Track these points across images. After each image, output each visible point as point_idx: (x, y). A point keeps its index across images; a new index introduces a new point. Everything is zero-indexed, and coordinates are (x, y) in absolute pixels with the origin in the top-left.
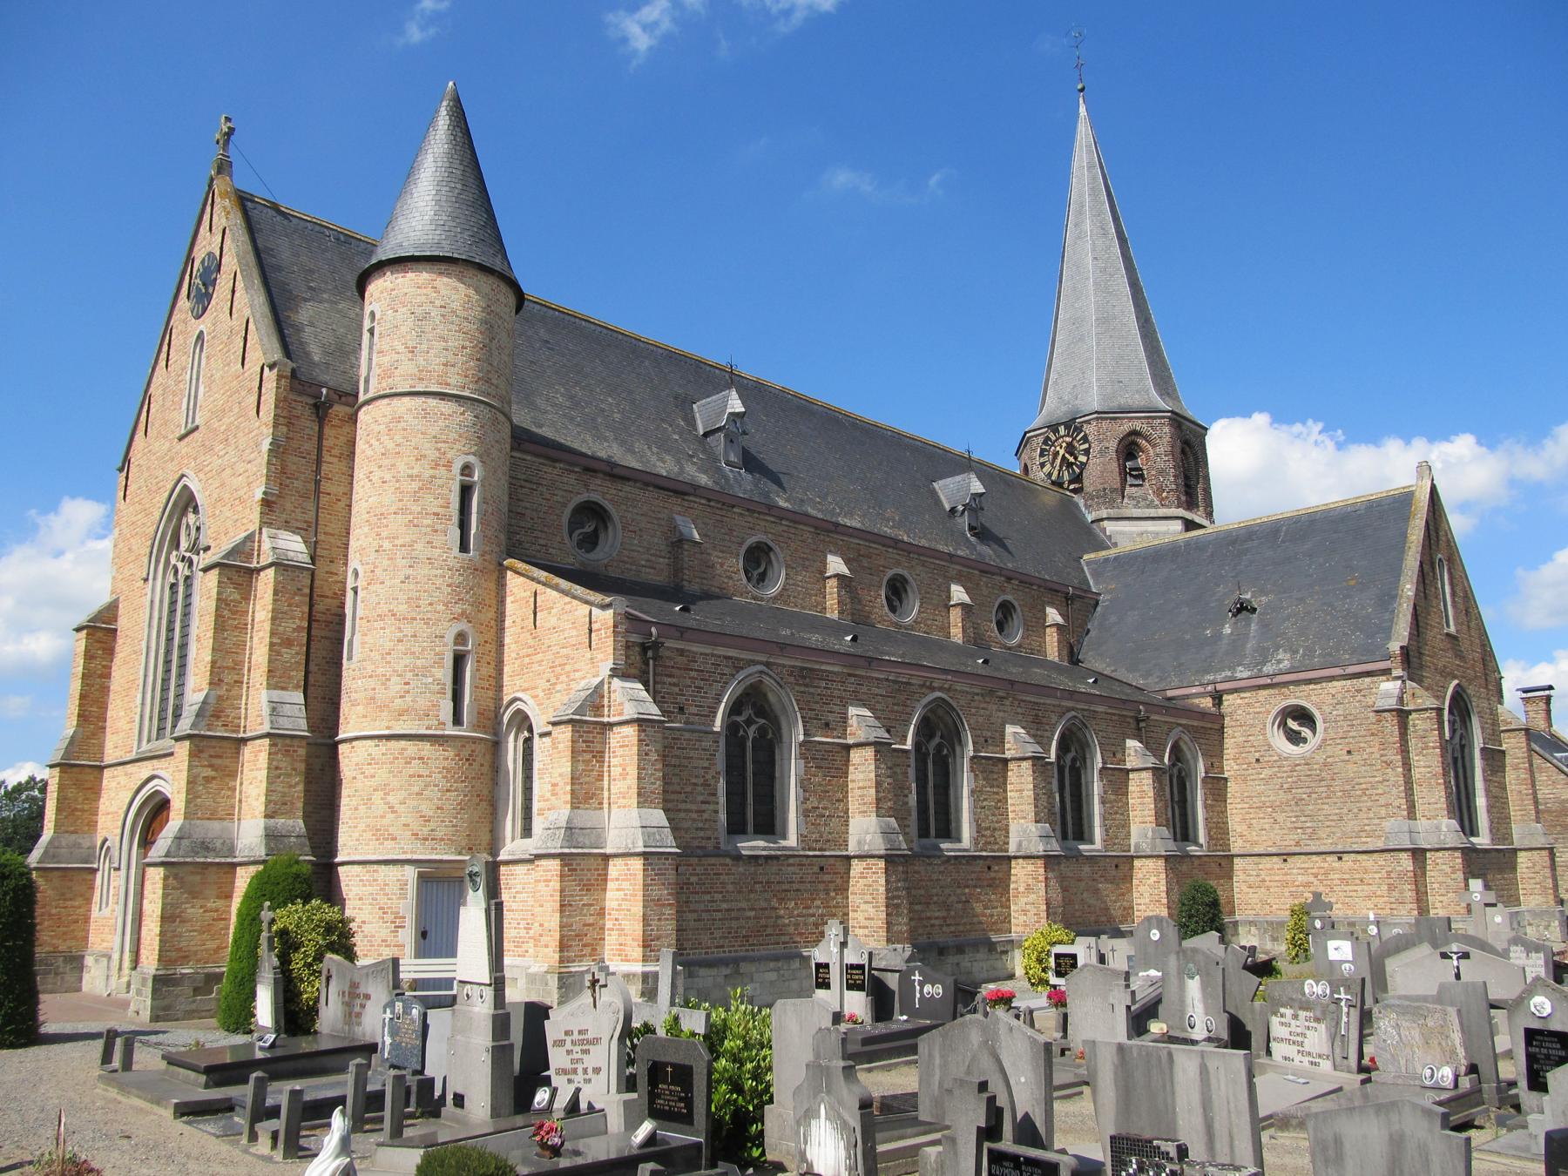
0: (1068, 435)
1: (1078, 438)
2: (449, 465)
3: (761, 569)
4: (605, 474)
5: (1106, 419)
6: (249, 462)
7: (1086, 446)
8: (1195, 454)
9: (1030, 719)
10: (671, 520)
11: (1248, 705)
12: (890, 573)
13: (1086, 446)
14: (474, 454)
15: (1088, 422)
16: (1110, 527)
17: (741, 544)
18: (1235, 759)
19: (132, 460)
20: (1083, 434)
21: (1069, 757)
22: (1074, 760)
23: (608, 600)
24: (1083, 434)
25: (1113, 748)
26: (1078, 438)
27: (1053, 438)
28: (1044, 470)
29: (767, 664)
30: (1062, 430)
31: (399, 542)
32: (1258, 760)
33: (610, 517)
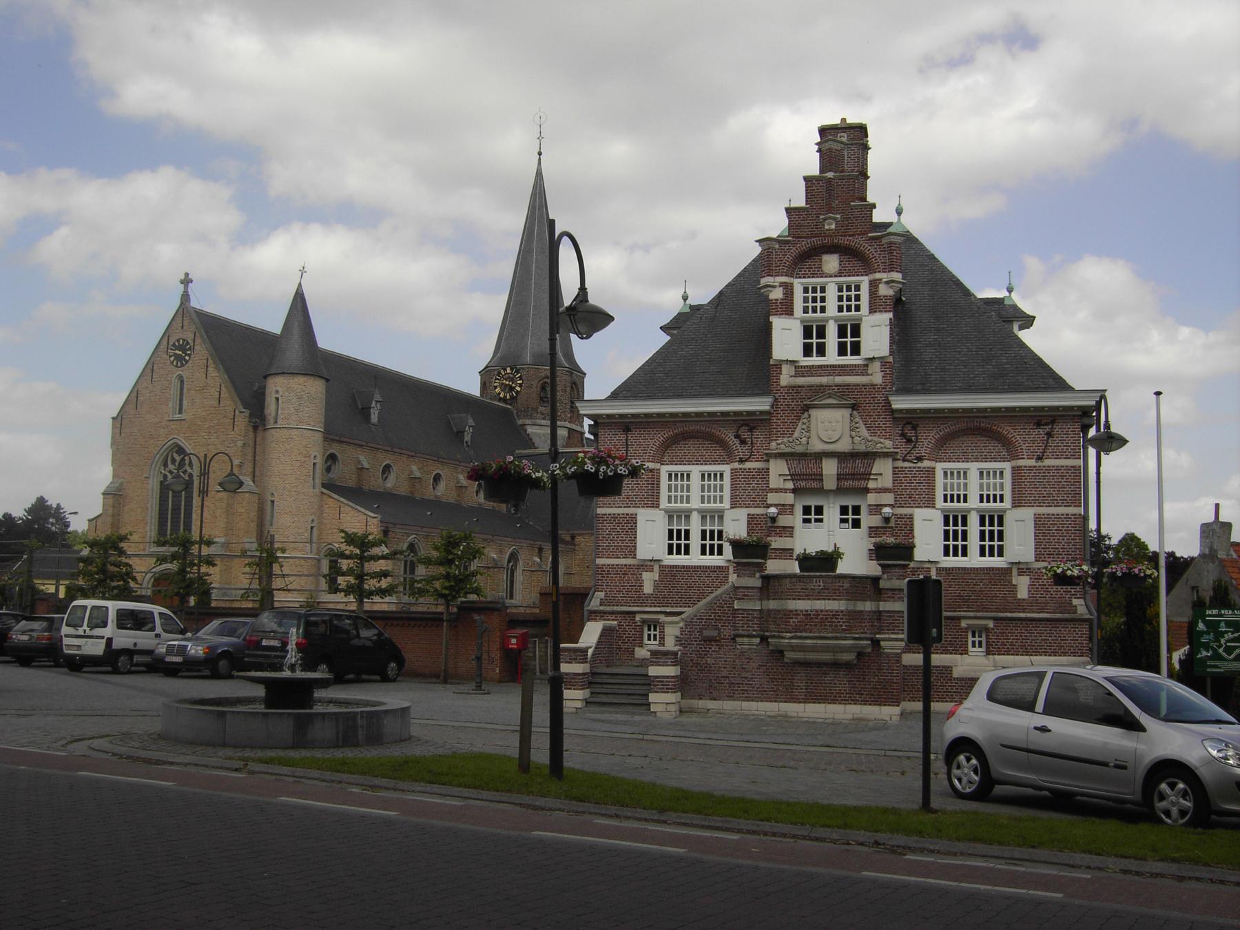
0: (511, 373)
1: (517, 376)
2: (310, 456)
3: (386, 475)
4: (337, 441)
5: (533, 368)
6: (228, 447)
7: (521, 382)
8: (578, 389)
9: (498, 550)
10: (357, 458)
11: (587, 542)
12: (435, 473)
13: (521, 382)
14: (318, 451)
15: (523, 369)
16: (530, 430)
17: (381, 466)
18: (578, 566)
19: (124, 417)
20: (519, 375)
21: (511, 564)
22: (512, 566)
23: (376, 515)
24: (519, 375)
25: (528, 561)
26: (517, 376)
27: (503, 374)
28: (496, 390)
29: (416, 534)
30: (509, 370)
31: (293, 485)
32: (588, 567)
33: (337, 459)
